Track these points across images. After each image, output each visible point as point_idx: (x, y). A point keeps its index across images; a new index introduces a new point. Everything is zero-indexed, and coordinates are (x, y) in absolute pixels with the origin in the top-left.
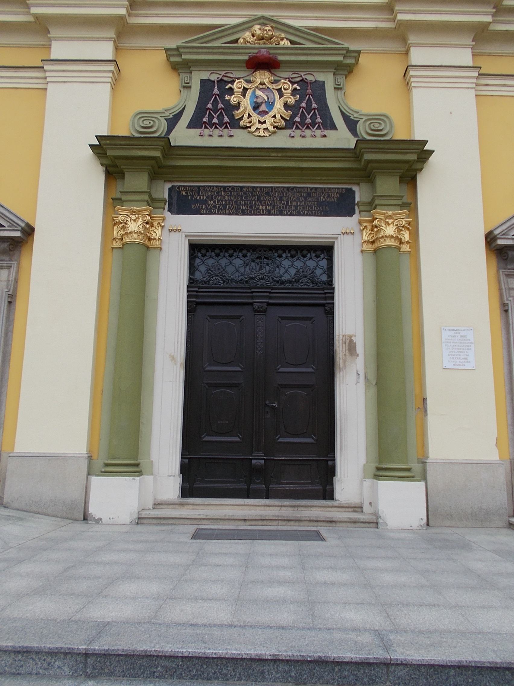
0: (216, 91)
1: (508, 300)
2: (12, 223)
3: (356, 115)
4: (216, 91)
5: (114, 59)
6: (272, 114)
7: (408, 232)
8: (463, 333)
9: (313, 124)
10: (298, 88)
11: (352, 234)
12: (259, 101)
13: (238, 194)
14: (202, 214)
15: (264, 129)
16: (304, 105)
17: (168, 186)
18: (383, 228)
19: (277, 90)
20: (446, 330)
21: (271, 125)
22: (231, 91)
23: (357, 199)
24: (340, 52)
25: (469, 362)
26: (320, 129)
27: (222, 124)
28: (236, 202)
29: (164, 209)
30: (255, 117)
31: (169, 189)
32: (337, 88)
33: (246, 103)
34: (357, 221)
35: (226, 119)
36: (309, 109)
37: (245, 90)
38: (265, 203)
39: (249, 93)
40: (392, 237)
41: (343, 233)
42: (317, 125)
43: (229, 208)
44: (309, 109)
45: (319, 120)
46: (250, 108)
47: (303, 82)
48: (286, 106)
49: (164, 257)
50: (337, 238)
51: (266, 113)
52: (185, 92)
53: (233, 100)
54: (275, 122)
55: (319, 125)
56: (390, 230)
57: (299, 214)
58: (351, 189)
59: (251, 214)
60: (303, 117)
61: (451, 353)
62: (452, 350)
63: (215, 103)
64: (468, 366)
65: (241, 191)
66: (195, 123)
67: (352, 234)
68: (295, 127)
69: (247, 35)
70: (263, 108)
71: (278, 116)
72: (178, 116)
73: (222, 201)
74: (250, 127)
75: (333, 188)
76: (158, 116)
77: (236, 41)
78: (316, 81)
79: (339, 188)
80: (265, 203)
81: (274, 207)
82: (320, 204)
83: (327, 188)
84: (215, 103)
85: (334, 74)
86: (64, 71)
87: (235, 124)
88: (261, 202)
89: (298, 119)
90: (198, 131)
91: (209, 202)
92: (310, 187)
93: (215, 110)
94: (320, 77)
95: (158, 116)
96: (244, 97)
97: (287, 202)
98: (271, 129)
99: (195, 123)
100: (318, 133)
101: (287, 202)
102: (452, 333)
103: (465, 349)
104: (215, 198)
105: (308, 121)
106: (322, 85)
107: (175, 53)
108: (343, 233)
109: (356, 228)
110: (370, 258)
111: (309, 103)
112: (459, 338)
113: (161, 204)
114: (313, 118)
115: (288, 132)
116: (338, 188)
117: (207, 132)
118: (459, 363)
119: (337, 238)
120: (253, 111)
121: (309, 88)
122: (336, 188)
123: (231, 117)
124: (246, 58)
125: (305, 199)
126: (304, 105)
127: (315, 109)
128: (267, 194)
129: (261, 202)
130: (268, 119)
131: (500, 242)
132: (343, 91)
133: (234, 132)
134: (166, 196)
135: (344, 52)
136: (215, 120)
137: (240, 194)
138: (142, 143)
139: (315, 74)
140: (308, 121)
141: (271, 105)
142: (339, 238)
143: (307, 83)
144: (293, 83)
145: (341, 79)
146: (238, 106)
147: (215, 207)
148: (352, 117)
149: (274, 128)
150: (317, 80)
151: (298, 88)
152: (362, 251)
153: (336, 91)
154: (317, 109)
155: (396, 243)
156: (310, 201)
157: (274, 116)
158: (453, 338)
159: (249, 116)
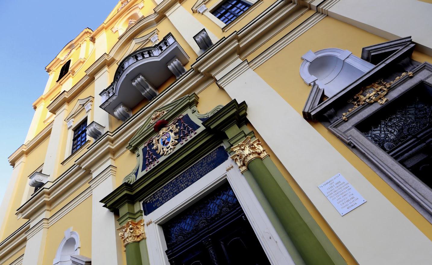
0: (148, 149)
1: (348, 140)
3: (206, 116)
6: (171, 141)
7: (260, 146)
8: (336, 181)
9: (189, 132)
10: (177, 124)
11: (232, 168)
12: (164, 140)
13: (171, 186)
14: (159, 207)
15: (170, 150)
17: (142, 202)
18: (243, 153)
19: (170, 131)
20: (322, 187)
21: (172, 145)
23: (225, 148)
24: (187, 99)
25: (358, 199)
26: (193, 132)
28: (171, 191)
29: (142, 216)
30: (165, 147)
33: (160, 145)
34: (231, 159)
37: (158, 140)
38: (184, 182)
39: (160, 140)
40: (250, 154)
41: (228, 170)
42: (191, 131)
43: (169, 195)
47: (179, 120)
49: (148, 241)
50: (226, 175)
51: (168, 143)
52: (138, 158)
54: (173, 144)
55: (192, 131)
56: (247, 151)
57: (202, 176)
58: (221, 147)
59: (180, 192)
61: (339, 201)
62: (338, 198)
65: (172, 184)
67: (232, 167)
68: (182, 139)
70: (166, 141)
71: (174, 140)
73: (165, 194)
74: (164, 153)
75: (211, 153)
76: (131, 175)
78: (183, 117)
79: (215, 150)
80: (184, 182)
81: (189, 182)
82: (209, 164)
83: (209, 154)
85: (190, 108)
86: (96, 182)
88: (182, 183)
91: (160, 199)
92: (201, 160)
93: (150, 156)
94: (184, 114)
96: (159, 143)
97: (194, 174)
101: (194, 174)
102: (328, 186)
103: (347, 191)
104: (162, 195)
106: (187, 116)
107: (130, 147)
108: (228, 170)
109: (233, 164)
110: (248, 173)
112: (336, 186)
113: (139, 214)
116: (214, 151)
118: (351, 204)
119: (226, 175)
120: (163, 146)
121: (182, 120)
122: (213, 151)
125: (201, 166)
127: (187, 126)
128: (183, 177)
129: (182, 183)
130: (169, 145)
131: (312, 114)
132: (197, 112)
135: (188, 98)
137: (171, 185)
138: (117, 192)
139: (182, 114)
142: (227, 175)
143: (180, 120)
145: (194, 108)
146: (157, 149)
147: (163, 199)
148: (205, 117)
149: (174, 145)
150: (184, 115)
151: (177, 124)
152: (242, 173)
153: (194, 114)
154: (188, 125)
155: (256, 155)
156: (204, 166)
157: (172, 141)
158: (331, 189)
159: (163, 149)
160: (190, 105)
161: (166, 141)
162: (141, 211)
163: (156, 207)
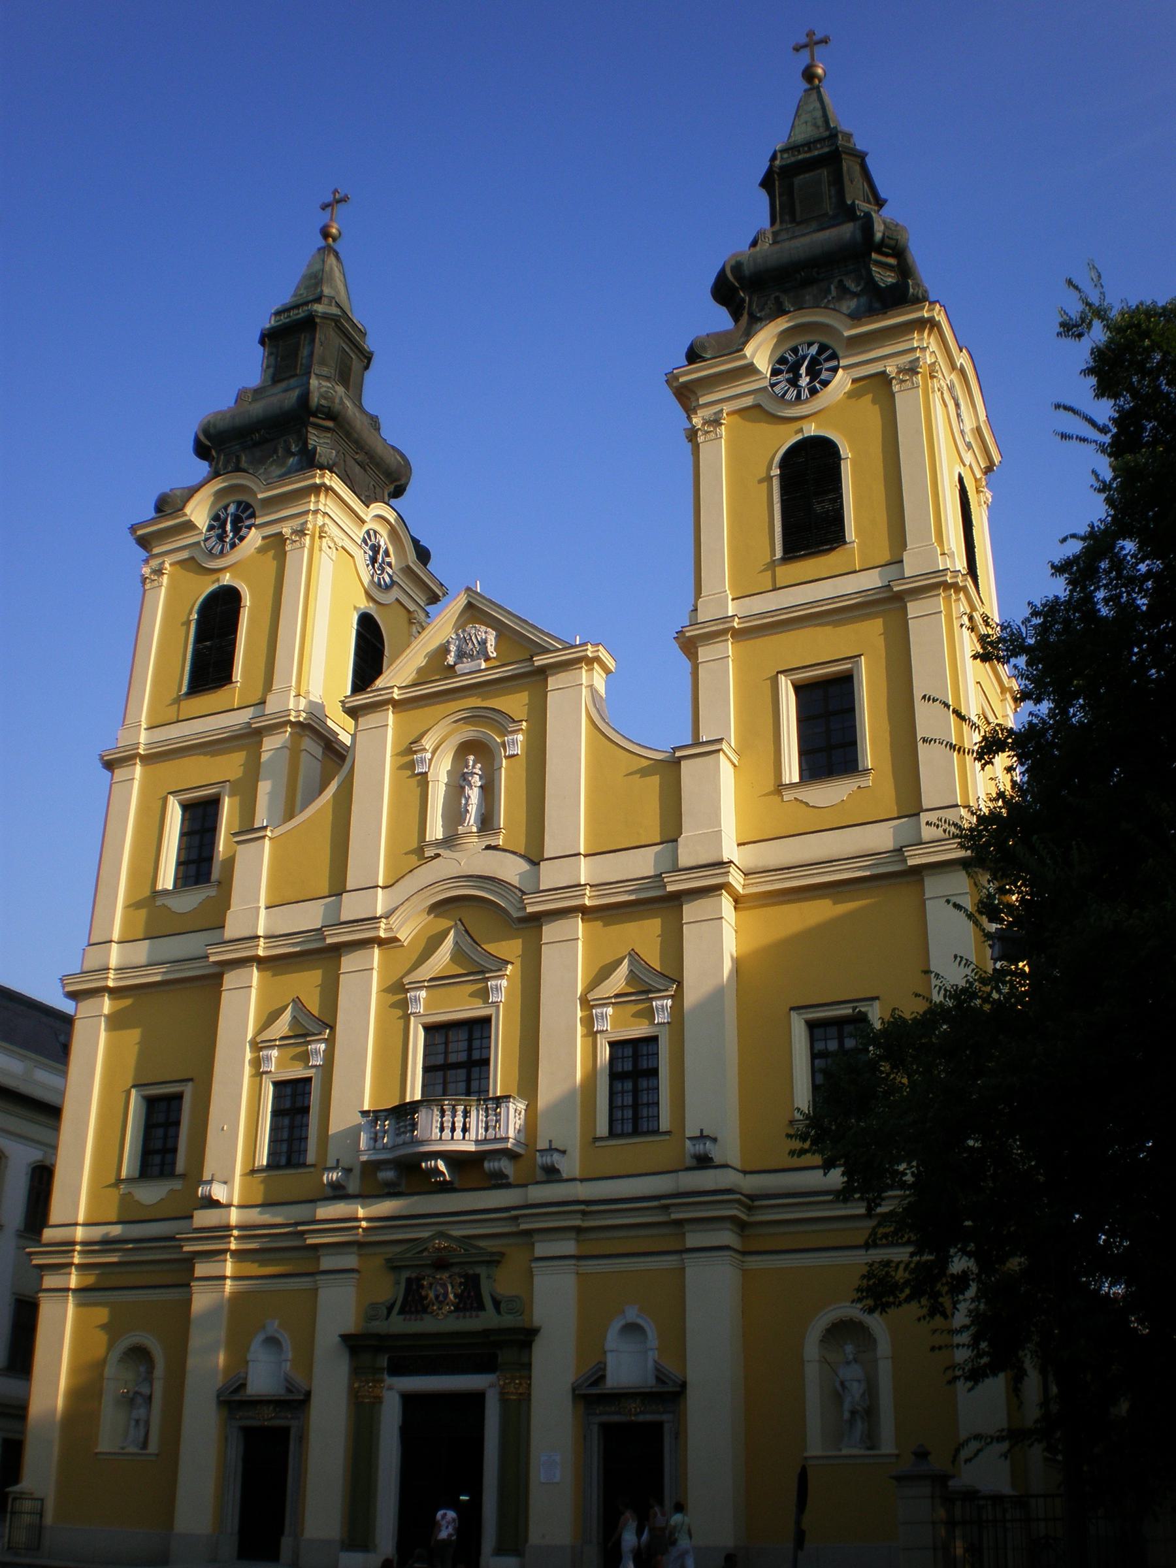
4: (414, 1287)
16: (466, 1294)
22: (422, 1286)
33: (432, 1295)
39: (434, 1286)
45: (475, 1305)
46: (434, 1299)
47: (466, 1276)
48: (456, 1296)
53: (423, 1293)
66: (402, 1312)
70: (441, 1298)
77: (426, 1249)
87: (425, 1310)
89: (461, 1306)
99: (402, 1312)
100: (474, 1313)
106: (477, 1277)
115: (455, 1314)
117: (408, 1317)
124: (429, 1262)
126: (466, 1294)
133: (424, 1316)
134: (385, 1365)
136: (413, 1309)
141: (446, 1294)
160: (488, 1263)
162: (384, 1369)
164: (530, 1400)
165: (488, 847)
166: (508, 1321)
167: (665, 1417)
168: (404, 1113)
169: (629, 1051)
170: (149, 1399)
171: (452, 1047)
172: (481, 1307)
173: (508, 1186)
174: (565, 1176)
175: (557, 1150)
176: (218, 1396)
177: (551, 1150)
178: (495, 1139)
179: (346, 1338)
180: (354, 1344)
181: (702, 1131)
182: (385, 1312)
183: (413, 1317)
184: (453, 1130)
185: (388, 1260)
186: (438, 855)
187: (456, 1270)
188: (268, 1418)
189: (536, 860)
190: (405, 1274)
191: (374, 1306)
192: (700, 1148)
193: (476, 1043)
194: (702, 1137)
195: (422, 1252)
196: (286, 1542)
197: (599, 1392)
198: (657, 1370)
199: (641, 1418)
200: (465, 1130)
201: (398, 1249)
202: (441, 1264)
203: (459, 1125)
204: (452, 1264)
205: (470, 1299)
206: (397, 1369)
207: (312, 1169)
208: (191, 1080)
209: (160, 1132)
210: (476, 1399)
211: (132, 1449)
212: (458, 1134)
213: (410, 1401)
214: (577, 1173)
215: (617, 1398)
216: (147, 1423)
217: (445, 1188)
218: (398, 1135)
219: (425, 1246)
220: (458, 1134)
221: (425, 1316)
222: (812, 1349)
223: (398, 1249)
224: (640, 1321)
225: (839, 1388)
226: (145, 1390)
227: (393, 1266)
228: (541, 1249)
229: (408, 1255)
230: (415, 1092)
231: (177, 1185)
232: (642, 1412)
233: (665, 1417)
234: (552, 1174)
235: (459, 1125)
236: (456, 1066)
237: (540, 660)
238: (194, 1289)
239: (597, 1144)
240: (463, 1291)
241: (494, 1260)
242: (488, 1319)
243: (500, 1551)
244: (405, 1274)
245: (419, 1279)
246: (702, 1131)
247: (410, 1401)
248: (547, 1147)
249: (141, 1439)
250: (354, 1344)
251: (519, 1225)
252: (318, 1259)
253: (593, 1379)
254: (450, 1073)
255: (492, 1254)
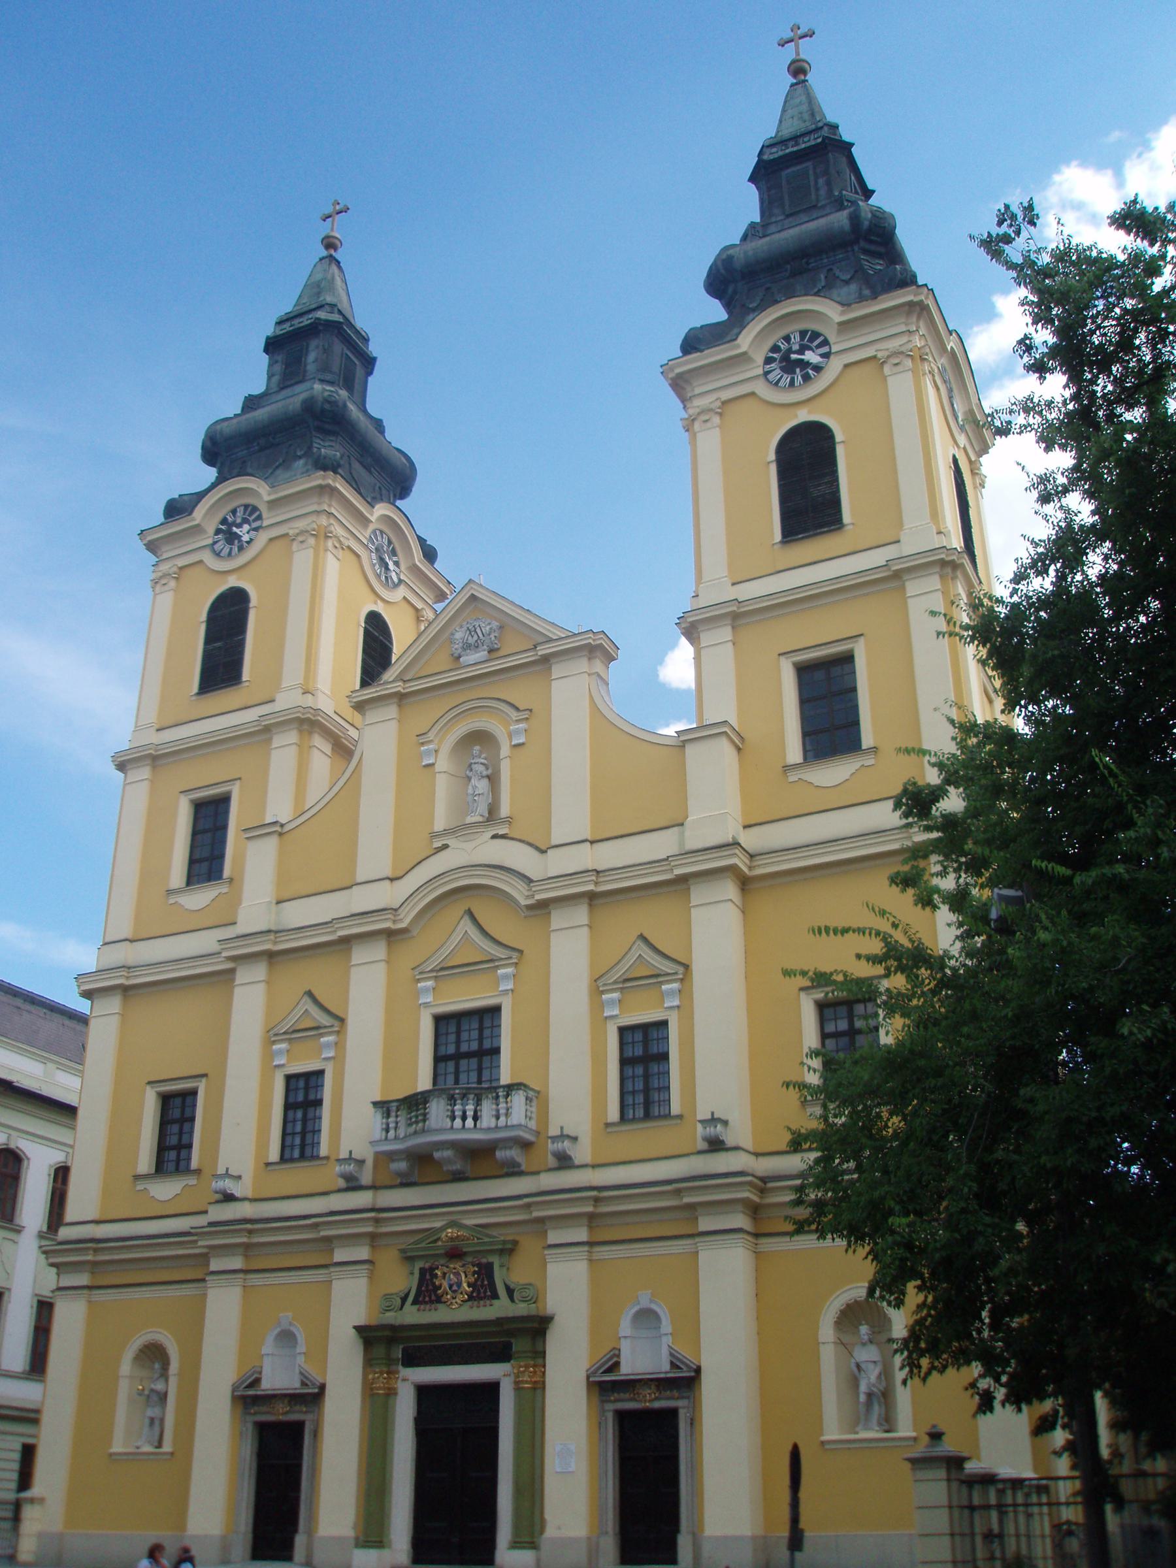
0: (428, 1277)
2: (314, 1384)
4: (428, 1277)
5: (370, 1258)
16: (479, 1283)
17: (401, 1347)
27: (431, 1302)
31: (403, 1350)
32: (502, 1266)
33: (445, 1284)
35: (433, 1298)
36: (482, 1286)
37: (444, 1274)
44: (482, 1286)
47: (479, 1265)
49: (399, 1398)
60: (479, 1292)
63: (427, 1285)
64: (570, 1470)
69: (443, 1235)
70: (455, 1288)
72: (407, 1295)
76: (394, 1296)
84: (427, 1285)
87: (439, 1300)
89: (475, 1294)
90: (417, 1306)
93: (427, 1291)
94: (491, 1260)
95: (394, 1296)
98: (459, 1302)
100: (488, 1302)
105: (482, 1295)
106: (490, 1266)
111: (483, 1282)
114: (485, 1292)
115: (470, 1303)
117: (422, 1307)
123: (436, 1295)
126: (479, 1283)
134: (400, 1356)
136: (427, 1299)
140: (482, 1295)
141: (459, 1284)
144: (474, 1266)
146: (440, 1287)
161: (455, 1288)
162: (398, 1359)
163: (418, 1365)
164: (544, 1388)
165: (495, 837)
166: (521, 1309)
167: (679, 1403)
168: (415, 1104)
169: (639, 1036)
170: (163, 1397)
171: (465, 1036)
172: (495, 1296)
173: (521, 1173)
174: (577, 1162)
175: (568, 1136)
176: (233, 1391)
177: (563, 1137)
178: (506, 1126)
179: (359, 1329)
180: (369, 1336)
181: (713, 1114)
182: (399, 1301)
183: (428, 1307)
184: (464, 1118)
185: (403, 1251)
186: (446, 847)
187: (469, 1259)
188: (281, 1413)
189: (544, 848)
190: (419, 1264)
191: (387, 1297)
192: (711, 1131)
193: (487, 1033)
194: (713, 1120)
195: (436, 1241)
196: (300, 1541)
197: (614, 1378)
198: (671, 1354)
199: (657, 1405)
200: (476, 1118)
201: (412, 1239)
202: (455, 1254)
203: (470, 1113)
204: (465, 1254)
205: (484, 1288)
206: (413, 1359)
207: (325, 1162)
208: (205, 1075)
209: (175, 1128)
210: (491, 1390)
211: (147, 1448)
212: (470, 1122)
213: (424, 1392)
214: (588, 1159)
215: (630, 1385)
216: (162, 1420)
217: (459, 1177)
218: (410, 1125)
219: (435, 1237)
220: (470, 1122)
221: (440, 1306)
222: (827, 1332)
223: (412, 1239)
224: (654, 1307)
225: (855, 1369)
226: (159, 1386)
227: (408, 1258)
228: (554, 1237)
229: (423, 1245)
230: (424, 1082)
231: (192, 1181)
232: (657, 1399)
233: (679, 1403)
234: (564, 1162)
235: (470, 1113)
236: (469, 1055)
237: (543, 650)
238: (209, 1284)
239: (609, 1130)
240: (476, 1280)
241: (509, 1250)
242: (501, 1308)
243: (516, 1544)
244: (419, 1264)
245: (432, 1269)
246: (713, 1114)
247: (424, 1392)
248: (559, 1133)
249: (156, 1437)
250: (369, 1336)
251: (531, 1212)
252: (332, 1251)
253: (606, 1366)
254: (463, 1063)
255: (504, 1242)
